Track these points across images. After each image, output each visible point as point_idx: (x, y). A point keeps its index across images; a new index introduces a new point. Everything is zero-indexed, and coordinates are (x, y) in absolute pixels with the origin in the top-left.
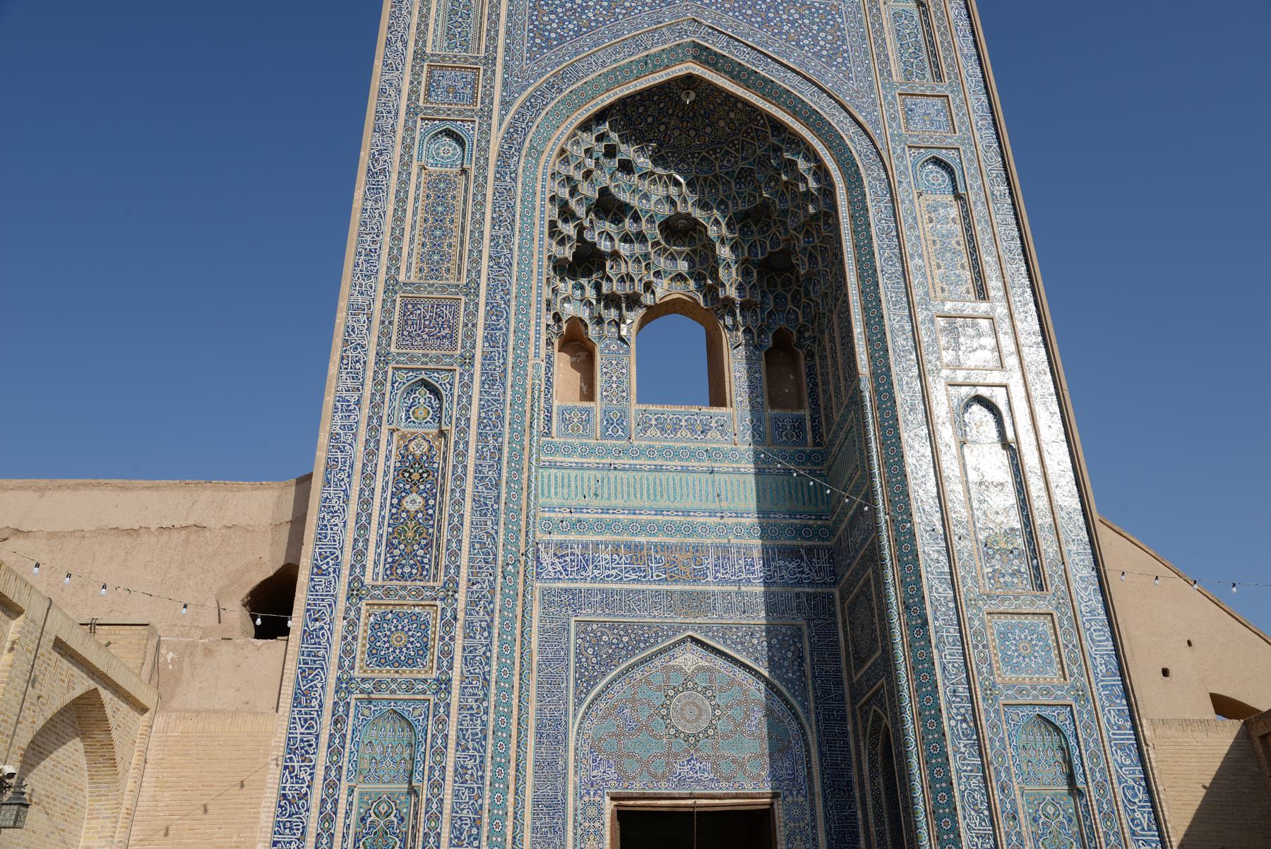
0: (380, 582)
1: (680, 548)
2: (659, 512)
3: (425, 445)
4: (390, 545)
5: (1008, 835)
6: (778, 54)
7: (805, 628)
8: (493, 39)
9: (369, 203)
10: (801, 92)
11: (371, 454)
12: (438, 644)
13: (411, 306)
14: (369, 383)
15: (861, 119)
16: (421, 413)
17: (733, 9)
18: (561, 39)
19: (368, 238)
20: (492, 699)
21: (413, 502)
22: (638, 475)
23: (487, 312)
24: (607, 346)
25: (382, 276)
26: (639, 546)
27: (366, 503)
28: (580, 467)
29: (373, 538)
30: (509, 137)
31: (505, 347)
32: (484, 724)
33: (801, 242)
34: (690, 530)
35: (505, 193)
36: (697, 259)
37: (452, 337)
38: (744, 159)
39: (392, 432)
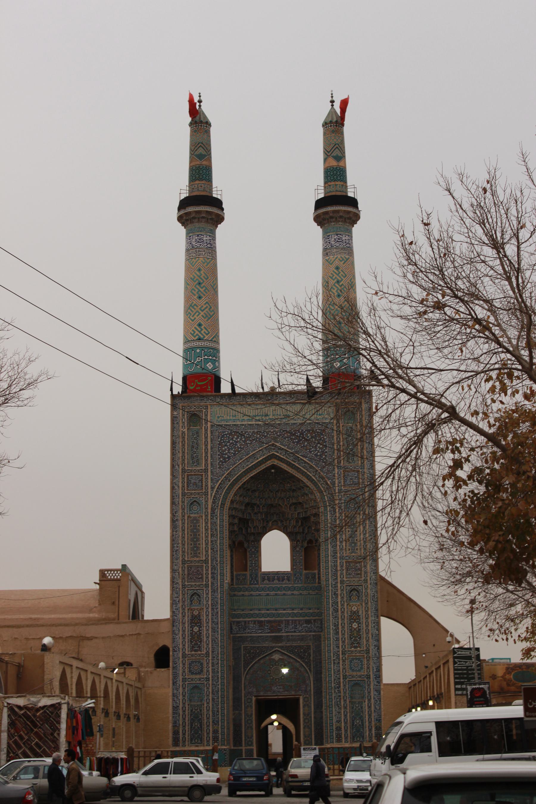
0: (190, 653)
1: (275, 621)
2: (268, 610)
3: (198, 612)
4: (191, 642)
5: (344, 712)
6: (302, 456)
7: (312, 646)
8: (206, 460)
9: (174, 532)
10: (310, 472)
11: (184, 616)
12: (206, 669)
13: (190, 567)
14: (181, 595)
15: (329, 483)
16: (196, 602)
17: (288, 437)
18: (229, 458)
19: (175, 545)
20: (220, 682)
21: (196, 629)
22: (261, 597)
23: (212, 569)
24: (251, 550)
25: (181, 559)
26: (262, 621)
27: (184, 631)
28: (243, 595)
29: (187, 640)
30: (214, 502)
31: (217, 580)
32: (218, 688)
33: (312, 519)
34: (279, 615)
35: (214, 524)
36: (281, 515)
37: (202, 578)
38: (294, 486)
39: (188, 609)
